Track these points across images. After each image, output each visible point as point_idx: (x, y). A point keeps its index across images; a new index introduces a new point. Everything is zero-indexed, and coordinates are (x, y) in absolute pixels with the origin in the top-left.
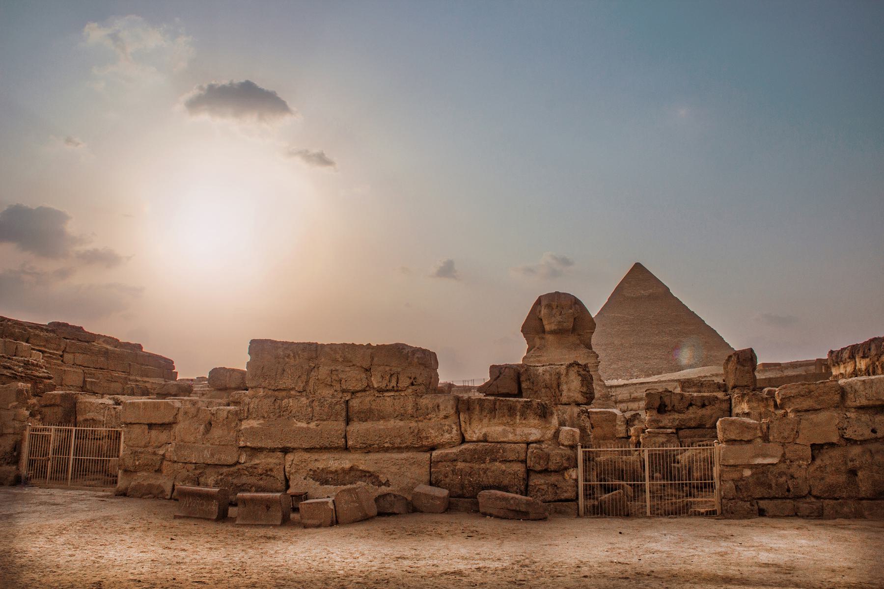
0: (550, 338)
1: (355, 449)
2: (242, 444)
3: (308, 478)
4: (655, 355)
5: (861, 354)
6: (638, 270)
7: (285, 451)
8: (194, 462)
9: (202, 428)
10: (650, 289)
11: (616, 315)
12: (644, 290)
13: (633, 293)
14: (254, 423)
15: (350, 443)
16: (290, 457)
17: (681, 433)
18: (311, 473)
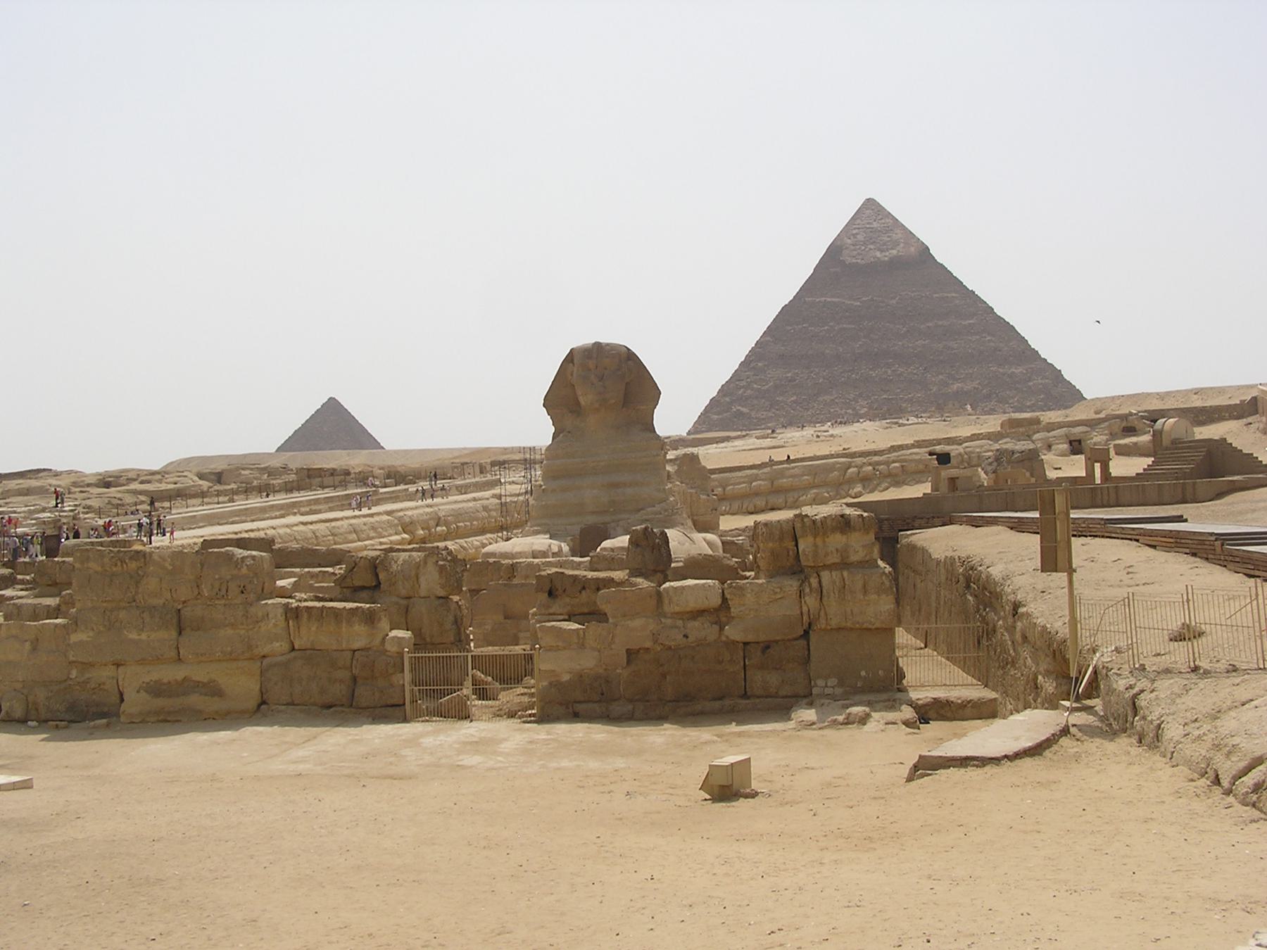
3: (142, 691)
4: (901, 375)
8: (21, 680)
9: (28, 645)
10: (892, 249)
11: (829, 299)
12: (882, 251)
13: (860, 257)
18: (144, 685)
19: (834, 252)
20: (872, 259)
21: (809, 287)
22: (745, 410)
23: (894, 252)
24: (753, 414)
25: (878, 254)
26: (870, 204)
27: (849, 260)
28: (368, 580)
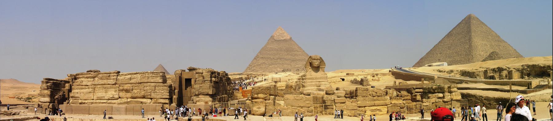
2: (358, 106)
4: (286, 63)
7: (365, 107)
19: (272, 37)
21: (268, 44)
24: (256, 69)
25: (281, 38)
27: (275, 39)
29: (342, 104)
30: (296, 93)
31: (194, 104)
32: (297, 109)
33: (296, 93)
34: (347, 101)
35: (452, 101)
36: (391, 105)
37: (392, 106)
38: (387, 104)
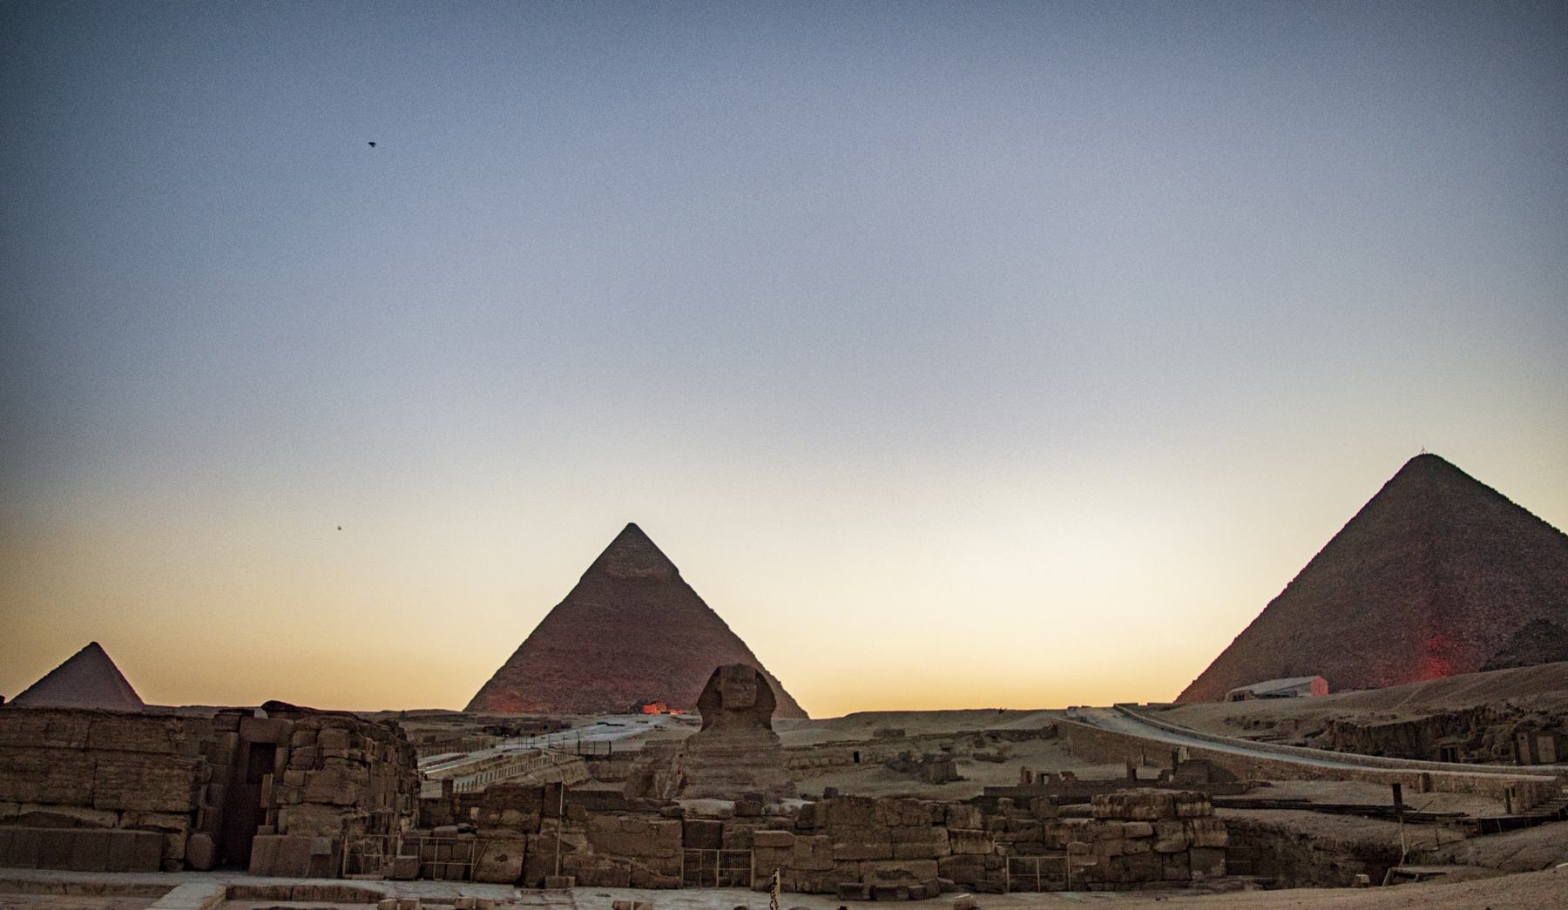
0: (729, 715)
1: (898, 859)
2: (835, 857)
5: (1118, 802)
6: (632, 529)
7: (859, 861)
9: (811, 849)
12: (640, 569)
14: (841, 845)
15: (896, 855)
16: (863, 865)
17: (1016, 845)
20: (632, 575)
22: (517, 693)
23: (650, 570)
25: (637, 571)
26: (632, 529)
28: (939, 818)
29: (780, 854)
30: (650, 808)
31: (279, 836)
32: (628, 863)
33: (650, 808)
34: (796, 842)
35: (1192, 852)
36: (950, 858)
37: (955, 860)
38: (935, 855)
